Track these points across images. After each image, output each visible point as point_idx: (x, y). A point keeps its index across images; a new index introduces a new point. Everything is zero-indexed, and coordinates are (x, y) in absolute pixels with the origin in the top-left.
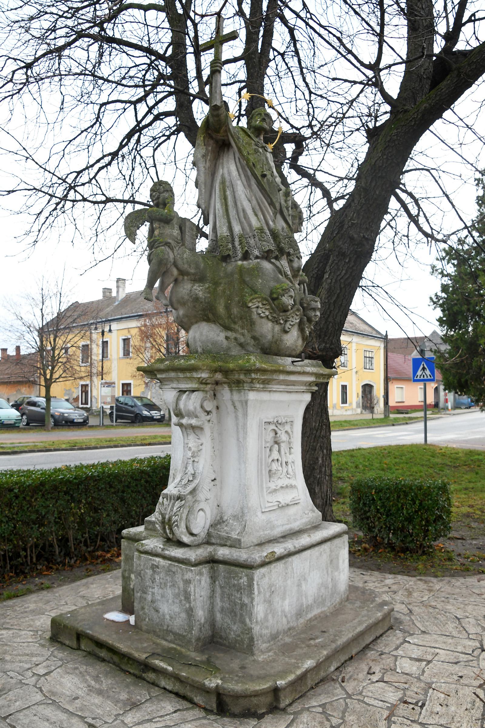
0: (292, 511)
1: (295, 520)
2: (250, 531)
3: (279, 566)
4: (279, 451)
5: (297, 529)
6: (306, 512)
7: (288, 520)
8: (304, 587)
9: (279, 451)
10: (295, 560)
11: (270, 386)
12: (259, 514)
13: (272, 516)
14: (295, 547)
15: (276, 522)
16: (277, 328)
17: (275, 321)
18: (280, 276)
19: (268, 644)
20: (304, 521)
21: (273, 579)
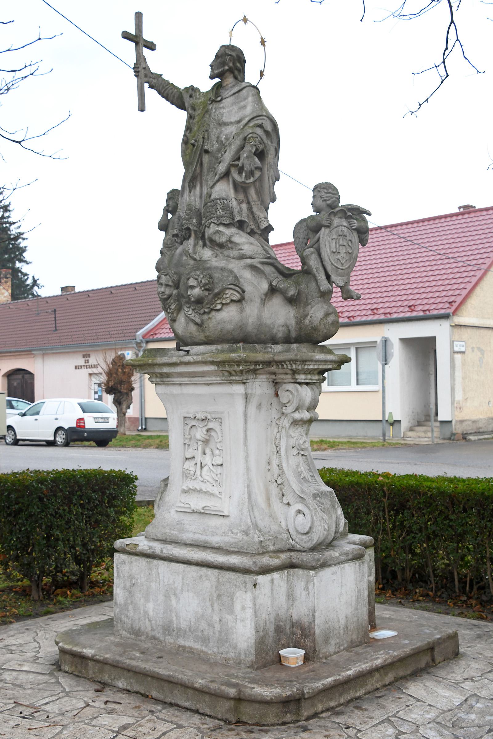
0: (214, 522)
1: (214, 534)
2: (157, 524)
3: (142, 562)
5: (217, 545)
6: (235, 531)
7: (204, 530)
8: (174, 601)
10: (163, 566)
11: (168, 379)
12: (173, 511)
13: (187, 519)
14: (162, 551)
15: (188, 527)
19: (129, 635)
20: (227, 539)
21: (133, 571)
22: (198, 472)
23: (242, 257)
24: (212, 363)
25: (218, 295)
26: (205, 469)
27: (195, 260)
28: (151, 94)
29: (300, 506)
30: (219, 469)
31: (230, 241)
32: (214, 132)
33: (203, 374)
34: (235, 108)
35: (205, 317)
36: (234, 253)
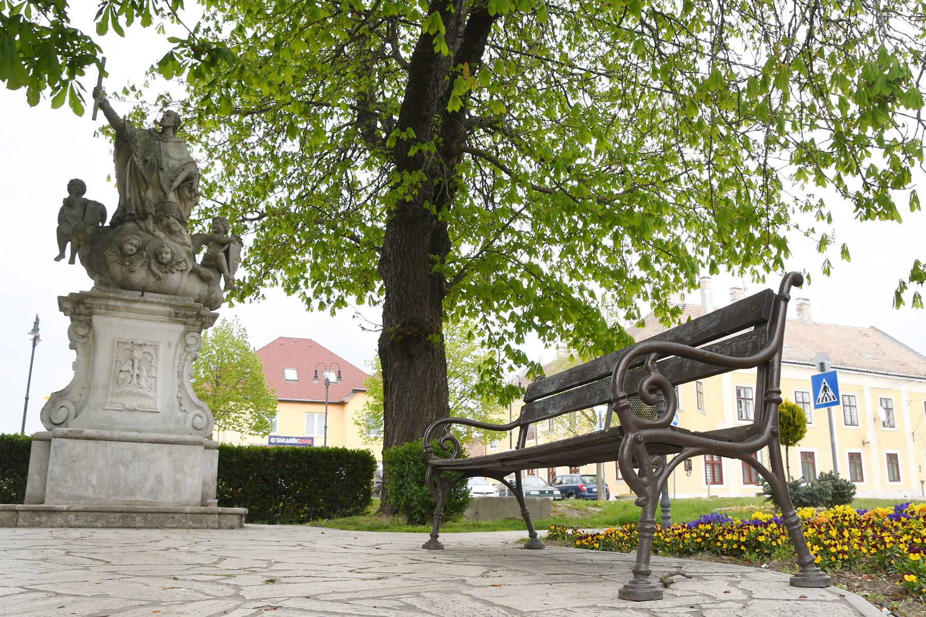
4: (133, 366)
9: (133, 366)
16: (125, 269)
17: (123, 264)
18: (141, 232)
22: (135, 380)
23: (184, 244)
24: (170, 305)
25: (178, 263)
26: (143, 379)
27: (154, 235)
28: (100, 113)
29: (198, 411)
30: (153, 380)
31: (180, 232)
32: (165, 160)
33: (152, 313)
34: (176, 152)
35: (164, 275)
36: (179, 240)
